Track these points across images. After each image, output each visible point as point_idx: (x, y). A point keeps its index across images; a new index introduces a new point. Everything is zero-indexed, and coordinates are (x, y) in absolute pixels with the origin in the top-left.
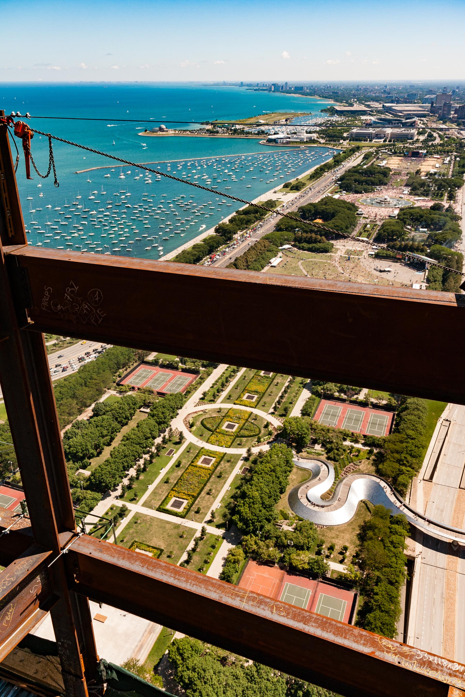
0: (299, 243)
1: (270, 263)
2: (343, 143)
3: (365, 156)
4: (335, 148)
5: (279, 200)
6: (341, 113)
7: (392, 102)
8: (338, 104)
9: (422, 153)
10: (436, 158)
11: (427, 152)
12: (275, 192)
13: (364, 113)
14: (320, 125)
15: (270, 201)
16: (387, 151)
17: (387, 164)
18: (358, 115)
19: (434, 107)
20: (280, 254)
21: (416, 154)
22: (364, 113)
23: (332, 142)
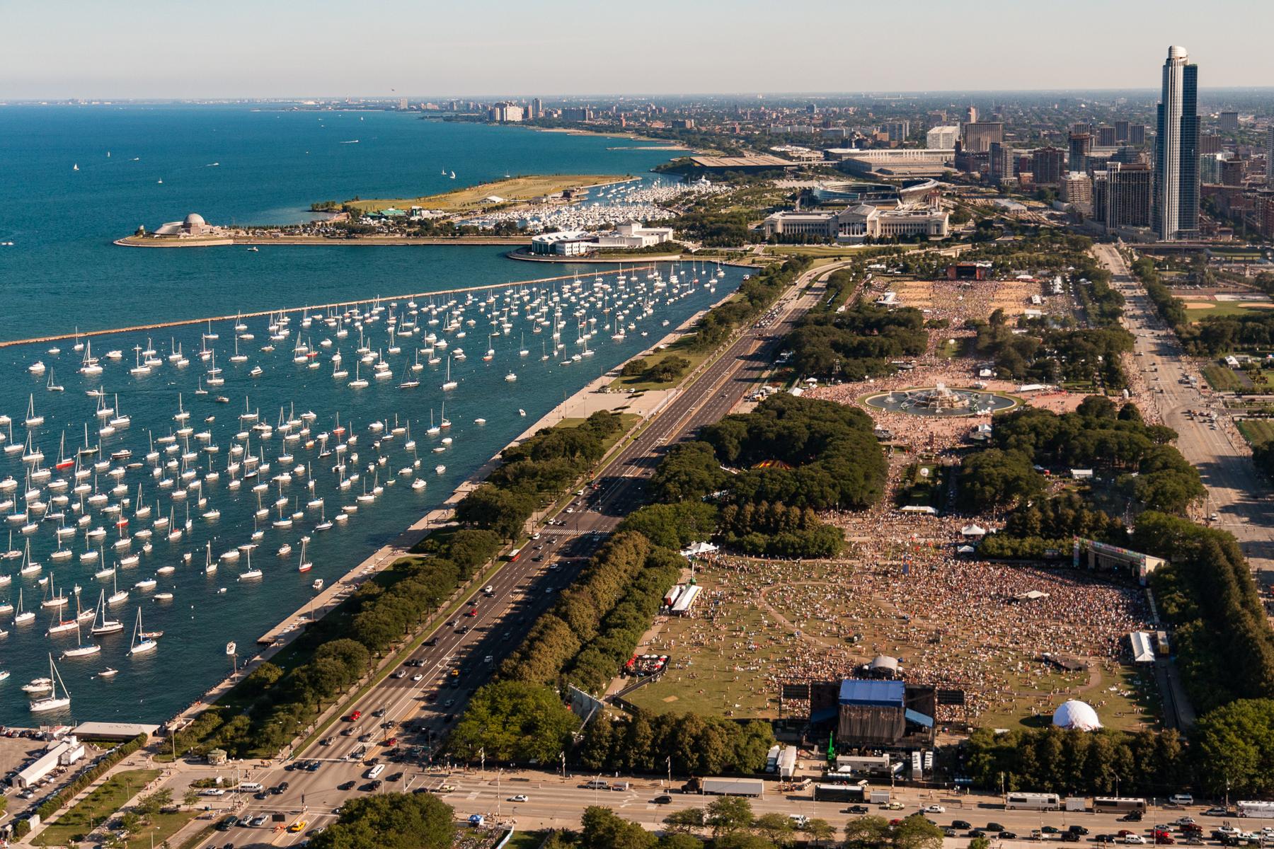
0: (739, 534)
1: (666, 601)
2: (752, 249)
3: (831, 278)
4: (732, 262)
5: (626, 411)
6: (718, 174)
7: (846, 144)
8: (701, 152)
9: (981, 268)
10: (1023, 280)
11: (994, 265)
12: (603, 389)
13: (779, 172)
14: (666, 205)
15: (602, 414)
16: (884, 266)
17: (897, 299)
18: (765, 177)
19: (964, 154)
20: (687, 574)
21: (965, 273)
22: (779, 172)
23: (720, 249)
